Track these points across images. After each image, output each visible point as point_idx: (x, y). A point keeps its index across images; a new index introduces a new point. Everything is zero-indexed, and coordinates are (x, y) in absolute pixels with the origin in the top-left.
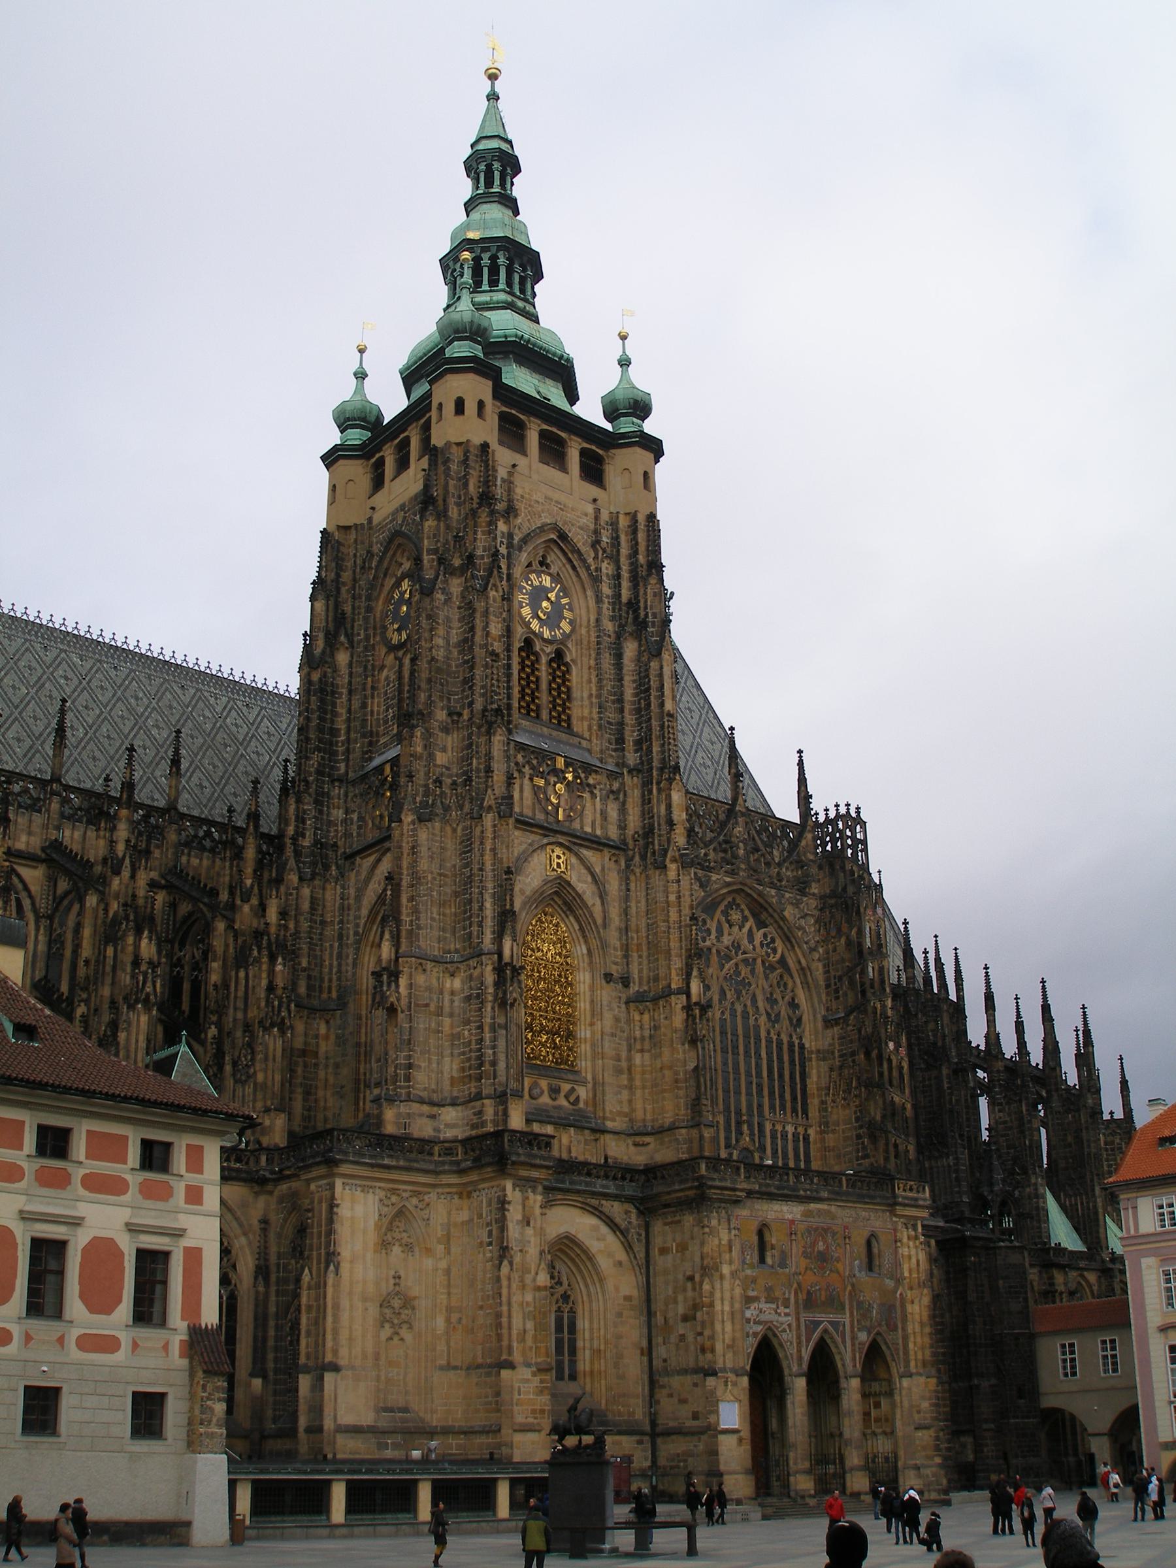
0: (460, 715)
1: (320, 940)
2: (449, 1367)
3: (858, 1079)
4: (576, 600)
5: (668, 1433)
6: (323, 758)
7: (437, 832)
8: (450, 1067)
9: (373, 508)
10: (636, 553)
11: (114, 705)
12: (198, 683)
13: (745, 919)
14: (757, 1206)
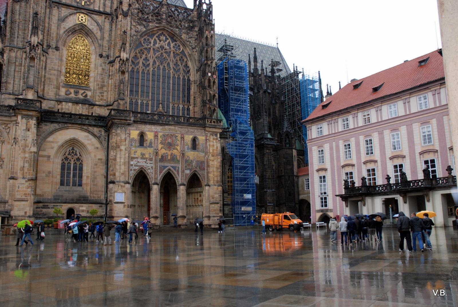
13: (167, 39)
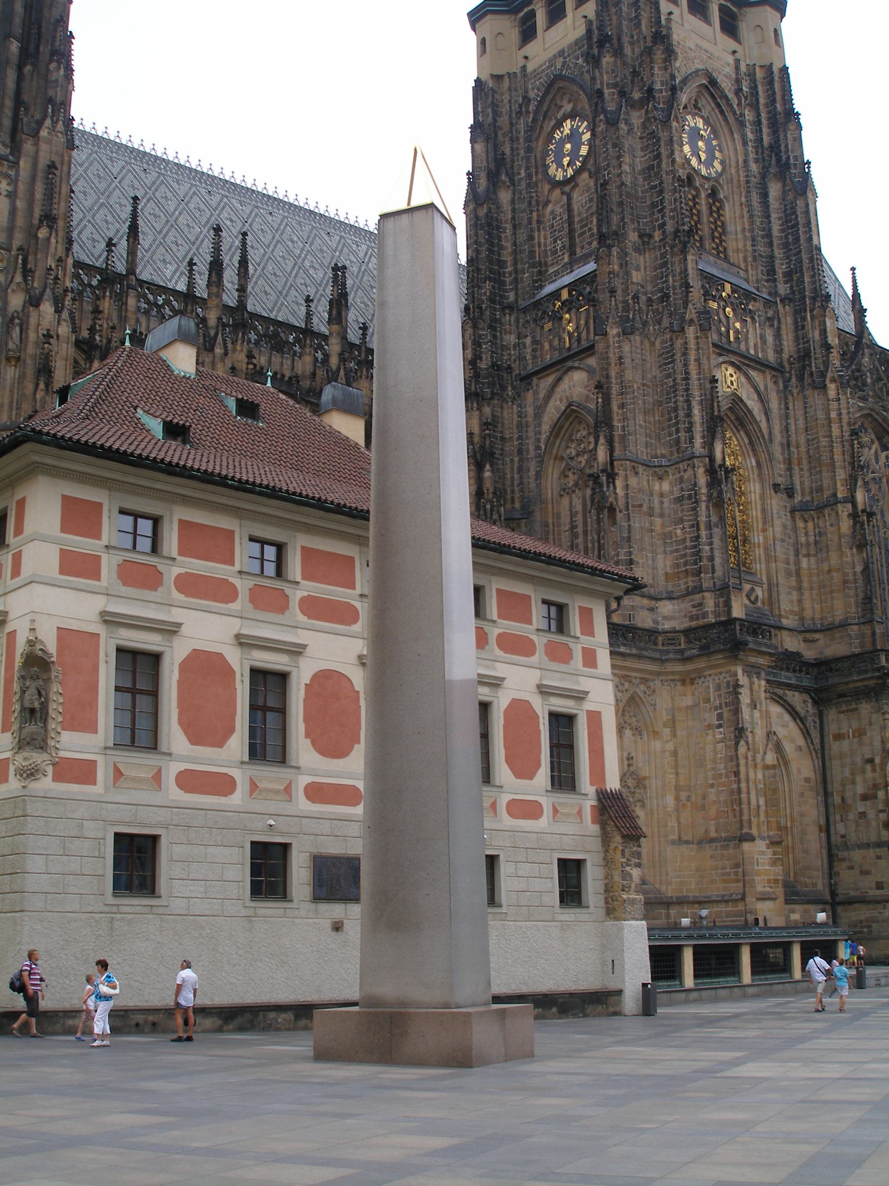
0: (650, 236)
1: (502, 454)
2: (680, 841)
4: (724, 143)
5: (850, 902)
6: (493, 287)
7: (638, 344)
8: (664, 563)
9: (526, 58)
10: (774, 101)
11: (275, 247)
12: (340, 231)
13: (872, 442)
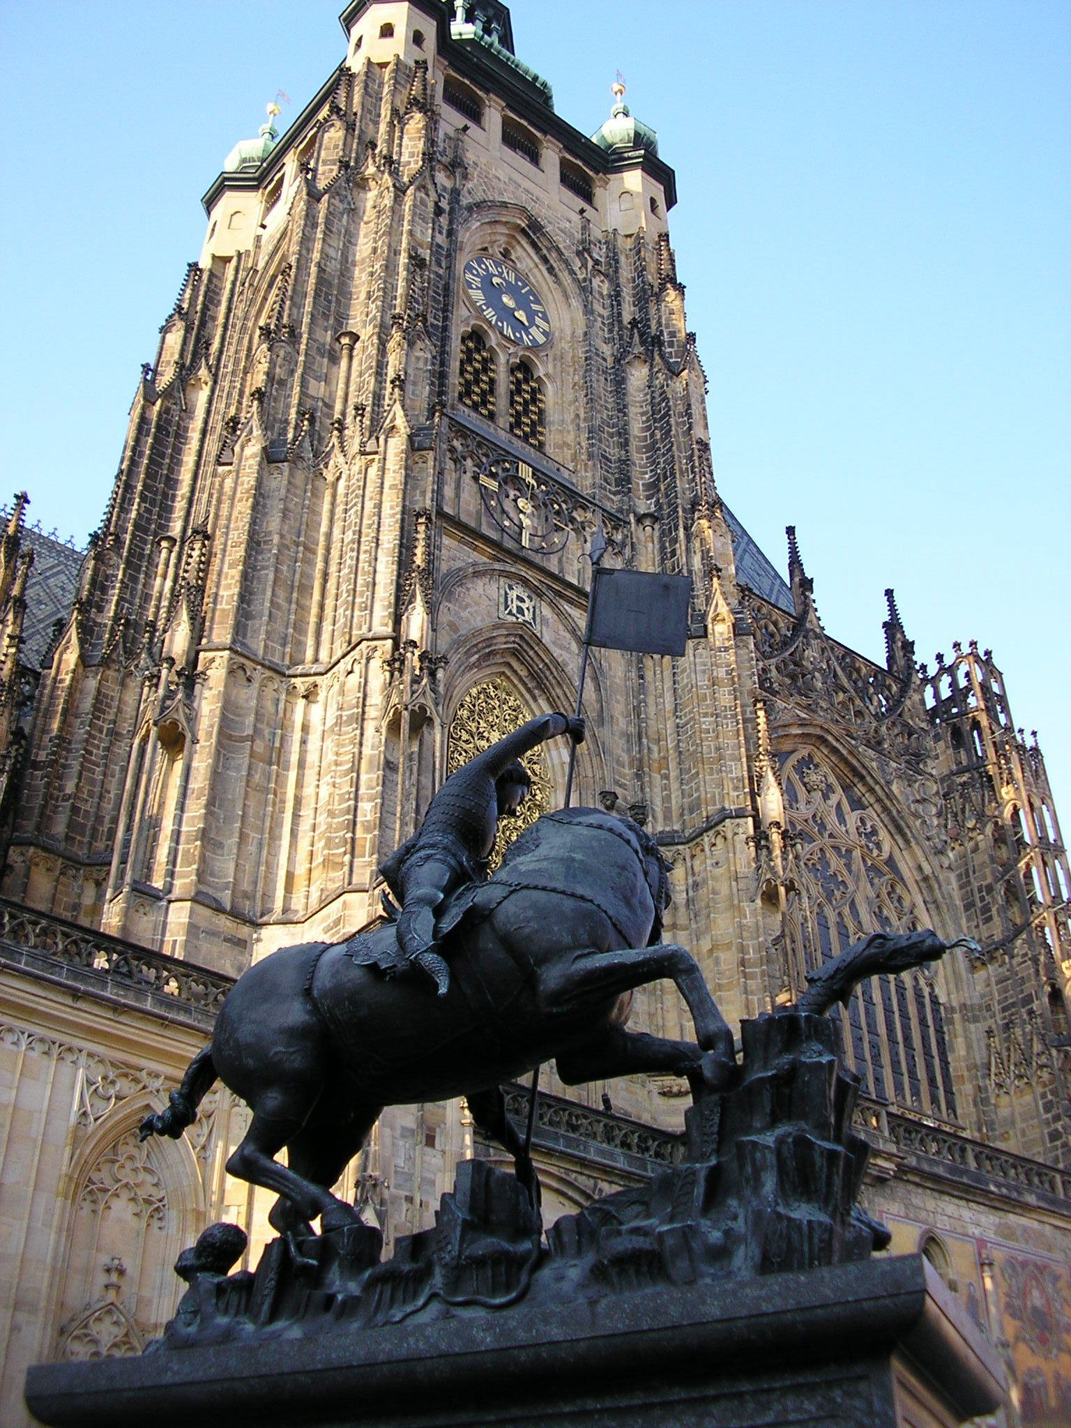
3: (1043, 1038)
6: (148, 511)
14: (916, 1201)
